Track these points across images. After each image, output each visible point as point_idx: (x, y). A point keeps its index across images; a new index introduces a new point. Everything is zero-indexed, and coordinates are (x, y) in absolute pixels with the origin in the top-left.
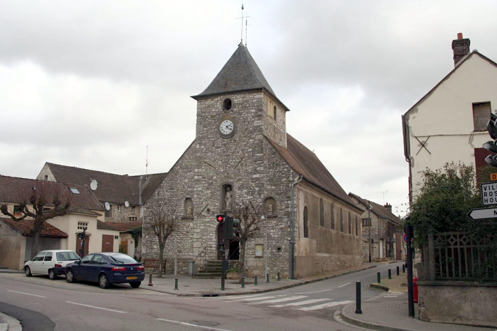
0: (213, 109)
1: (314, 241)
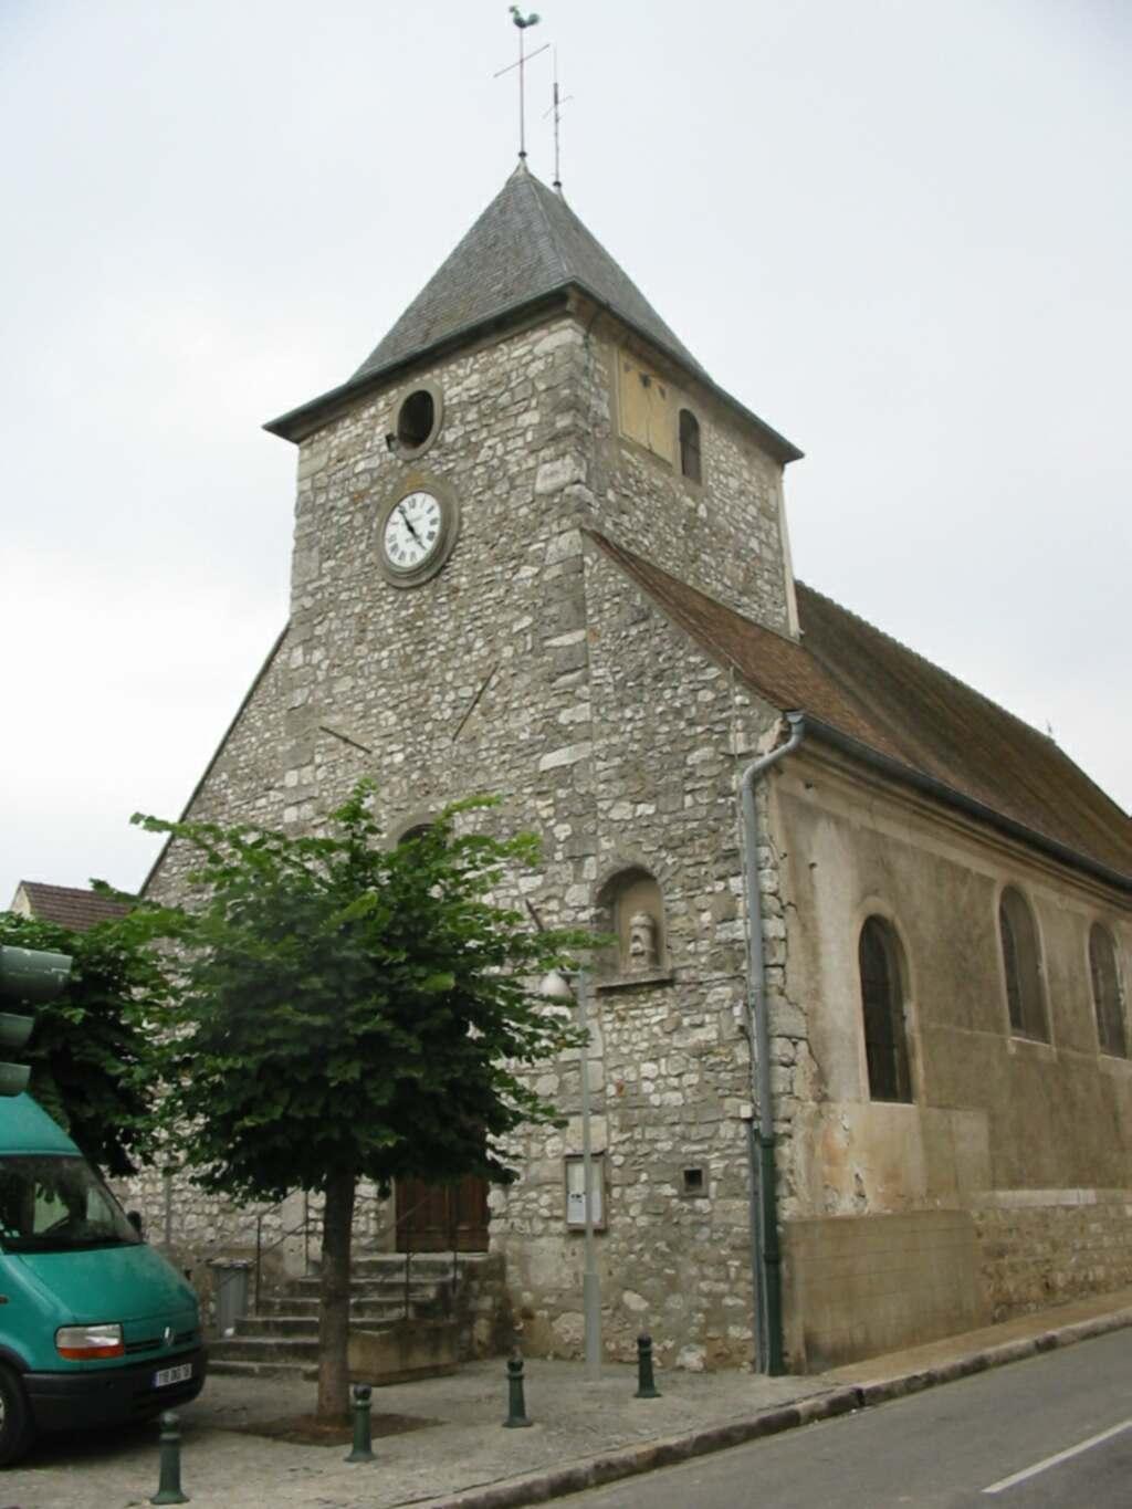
0: (356, 462)
1: (971, 1130)
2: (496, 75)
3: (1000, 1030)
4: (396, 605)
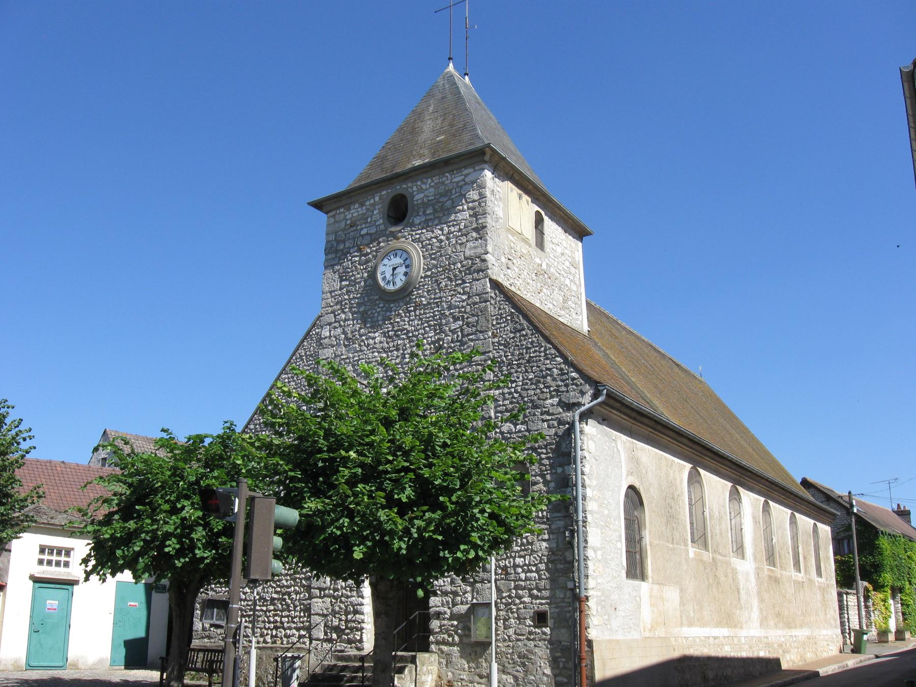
0: (362, 229)
1: (672, 595)
2: (436, 12)
3: (686, 545)
4: (384, 309)
